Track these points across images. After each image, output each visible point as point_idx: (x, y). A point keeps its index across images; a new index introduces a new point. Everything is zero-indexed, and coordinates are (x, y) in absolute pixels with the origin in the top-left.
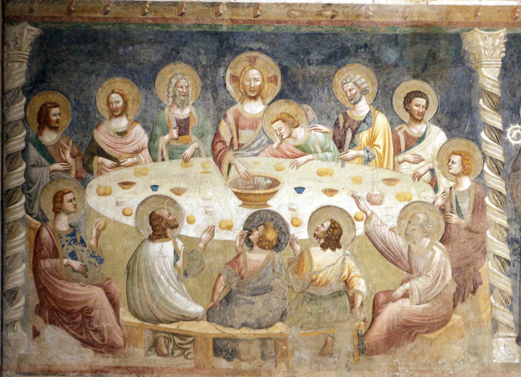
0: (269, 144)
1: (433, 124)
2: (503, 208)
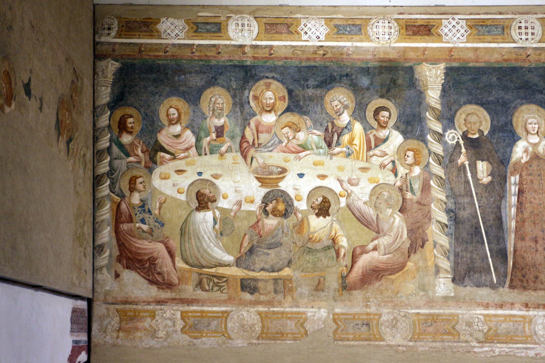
2: (443, 188)
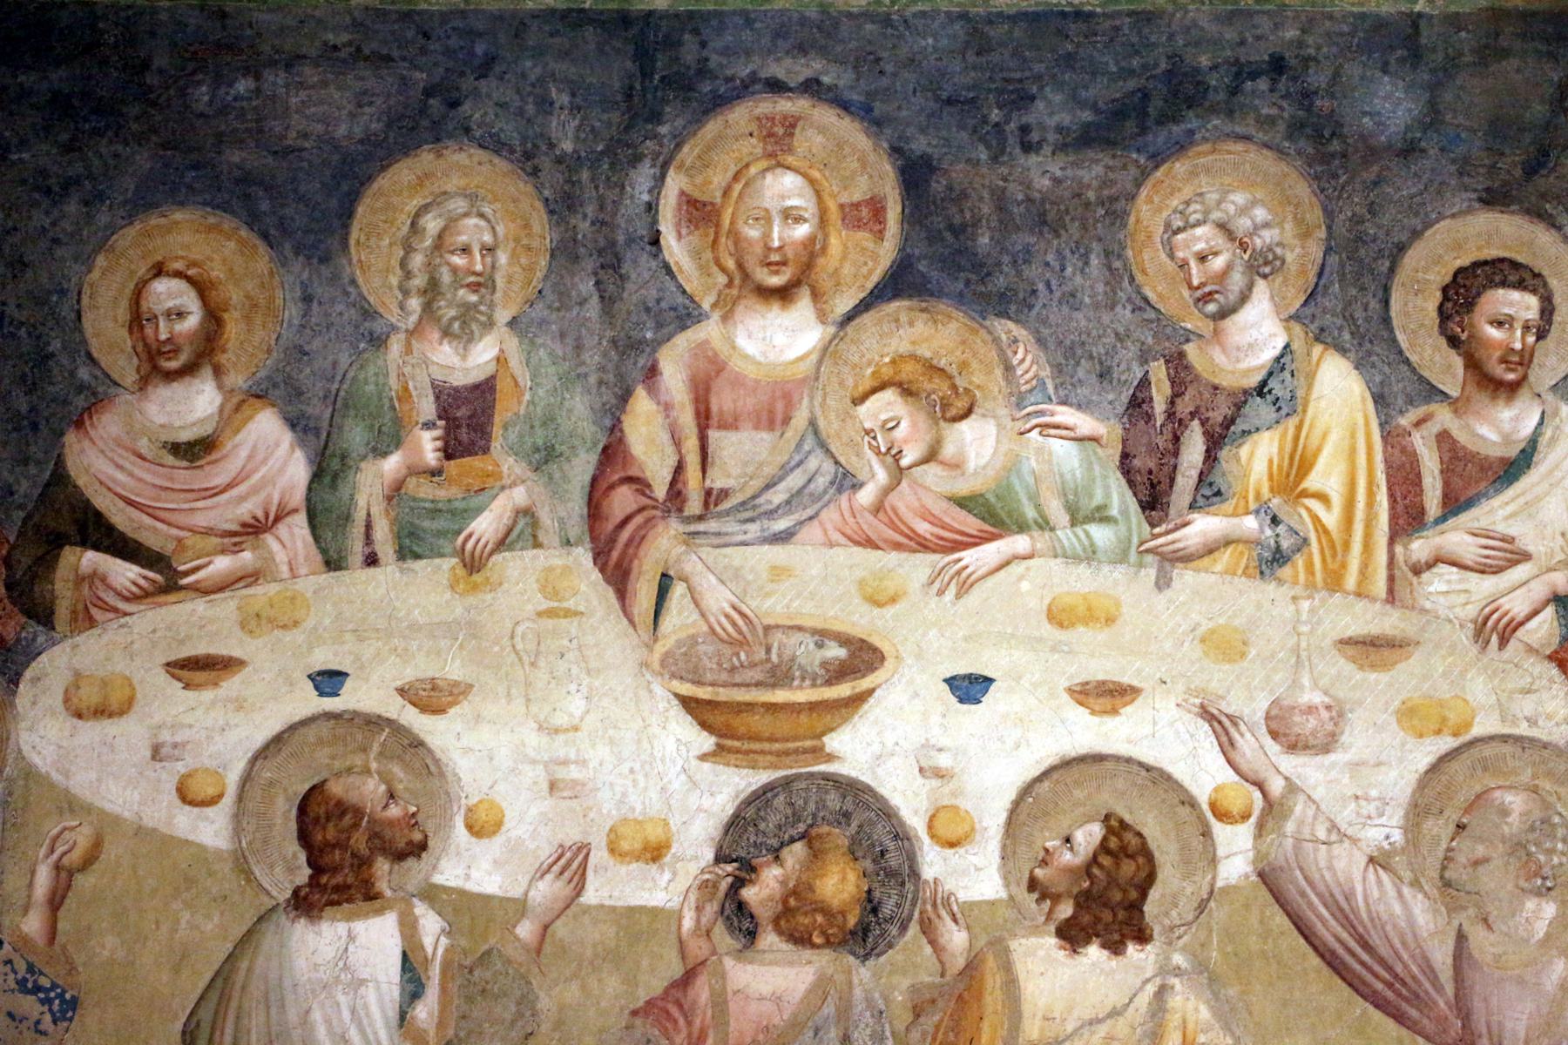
0: (840, 490)
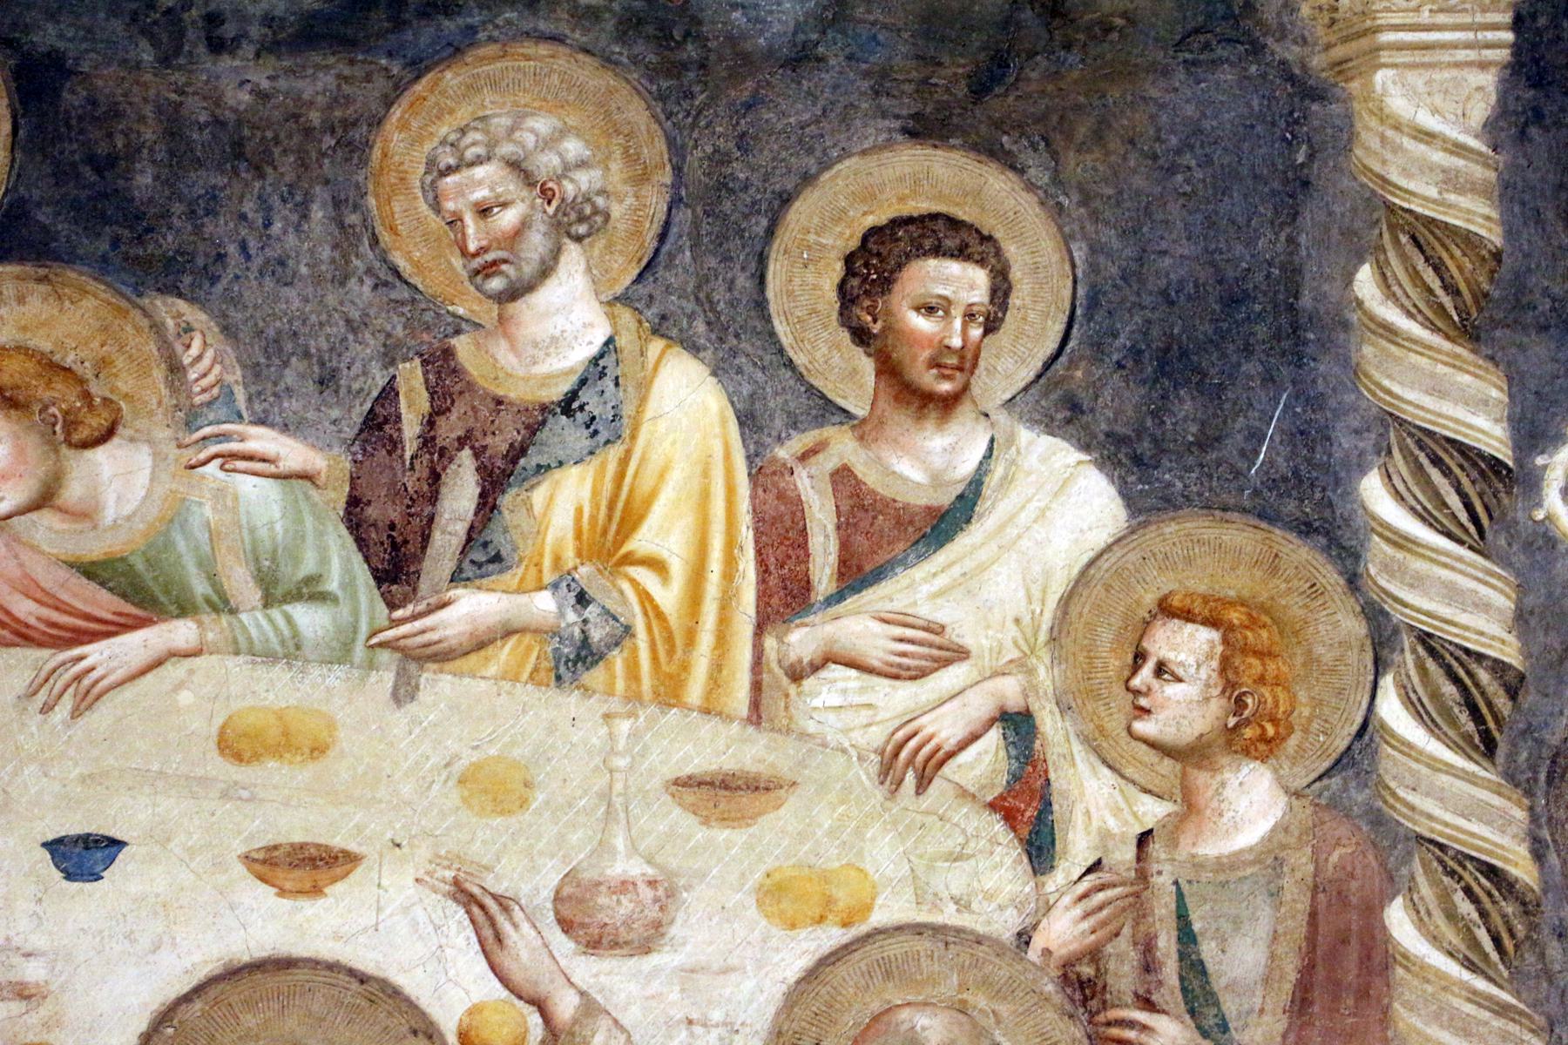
1: (1032, 422)
2: (1516, 980)
